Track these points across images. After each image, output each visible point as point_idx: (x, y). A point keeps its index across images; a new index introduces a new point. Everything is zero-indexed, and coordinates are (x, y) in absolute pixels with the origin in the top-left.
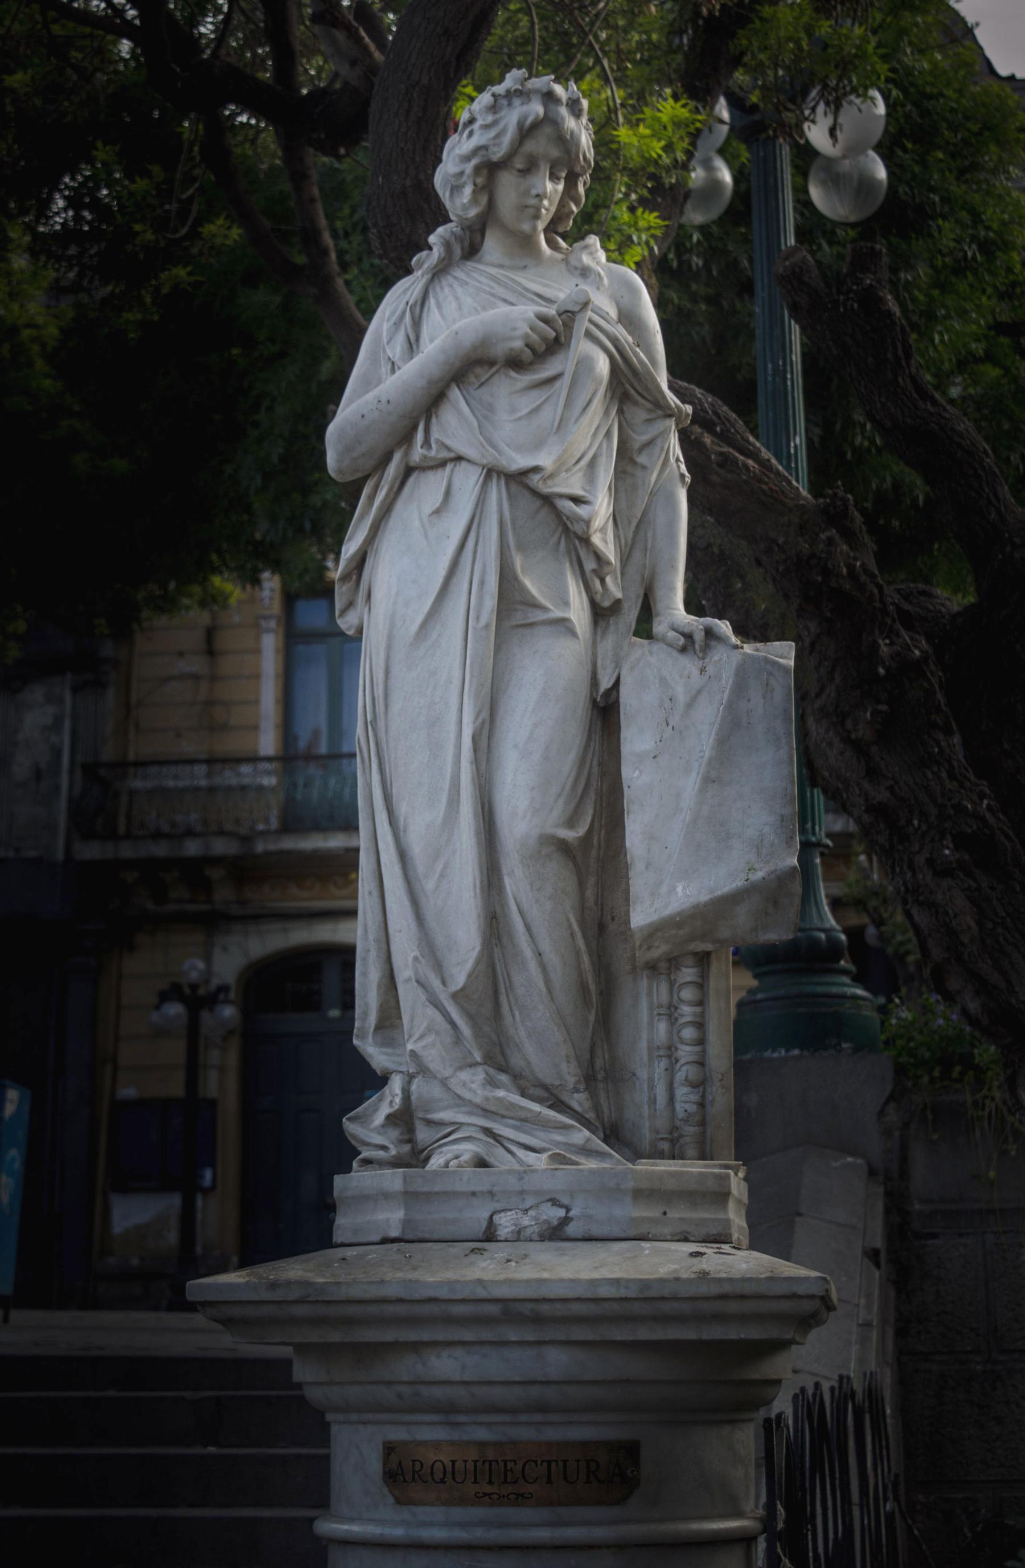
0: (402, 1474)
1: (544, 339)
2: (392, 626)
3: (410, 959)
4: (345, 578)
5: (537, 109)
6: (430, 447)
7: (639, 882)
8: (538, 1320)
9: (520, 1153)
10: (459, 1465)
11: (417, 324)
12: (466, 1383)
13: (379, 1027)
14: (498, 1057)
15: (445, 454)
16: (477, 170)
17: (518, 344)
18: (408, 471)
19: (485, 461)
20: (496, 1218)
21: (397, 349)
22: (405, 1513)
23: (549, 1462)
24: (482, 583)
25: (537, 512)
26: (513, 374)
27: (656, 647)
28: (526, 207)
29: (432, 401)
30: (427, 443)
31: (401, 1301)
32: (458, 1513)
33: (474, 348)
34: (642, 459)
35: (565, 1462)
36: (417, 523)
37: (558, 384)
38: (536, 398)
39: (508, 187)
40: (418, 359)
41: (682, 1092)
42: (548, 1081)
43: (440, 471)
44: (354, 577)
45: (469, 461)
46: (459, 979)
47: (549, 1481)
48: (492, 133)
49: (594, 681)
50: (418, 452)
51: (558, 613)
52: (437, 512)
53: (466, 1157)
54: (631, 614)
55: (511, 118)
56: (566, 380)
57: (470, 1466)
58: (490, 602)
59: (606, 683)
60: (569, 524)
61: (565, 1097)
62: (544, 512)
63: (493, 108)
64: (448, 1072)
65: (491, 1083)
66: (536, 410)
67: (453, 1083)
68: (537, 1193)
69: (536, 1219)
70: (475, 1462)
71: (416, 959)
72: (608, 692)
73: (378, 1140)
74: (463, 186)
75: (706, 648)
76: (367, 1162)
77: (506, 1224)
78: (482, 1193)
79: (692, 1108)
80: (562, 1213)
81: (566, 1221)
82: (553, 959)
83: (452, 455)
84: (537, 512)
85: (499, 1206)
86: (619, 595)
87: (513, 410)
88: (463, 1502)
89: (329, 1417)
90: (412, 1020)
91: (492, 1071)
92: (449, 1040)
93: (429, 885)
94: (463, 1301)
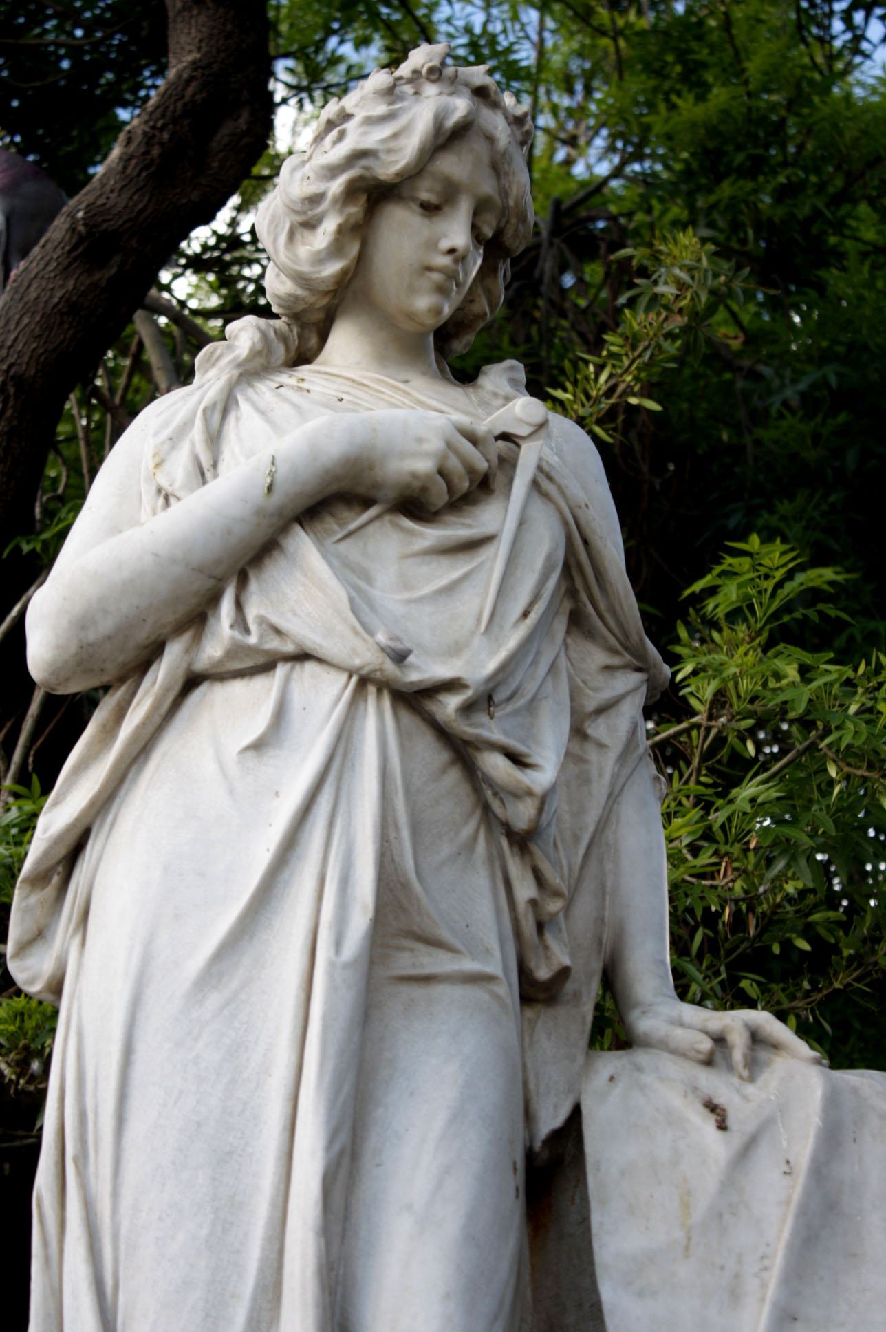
1: (471, 470)
4: (40, 879)
6: (247, 631)
11: (214, 439)
15: (274, 644)
16: (351, 192)
18: (192, 682)
19: (357, 662)
21: (179, 467)
25: (443, 771)
26: (407, 523)
28: (429, 269)
29: (251, 554)
30: (241, 622)
34: (598, 729)
36: (209, 767)
37: (485, 553)
43: (259, 682)
44: (56, 879)
45: (320, 660)
48: (385, 131)
50: (213, 649)
52: (258, 746)
55: (424, 112)
56: (500, 550)
59: (551, 1119)
60: (496, 806)
62: (454, 775)
63: (390, 93)
66: (450, 589)
72: (557, 1136)
74: (311, 225)
75: (753, 1066)
83: (289, 648)
84: (443, 771)
86: (566, 961)
87: (405, 584)
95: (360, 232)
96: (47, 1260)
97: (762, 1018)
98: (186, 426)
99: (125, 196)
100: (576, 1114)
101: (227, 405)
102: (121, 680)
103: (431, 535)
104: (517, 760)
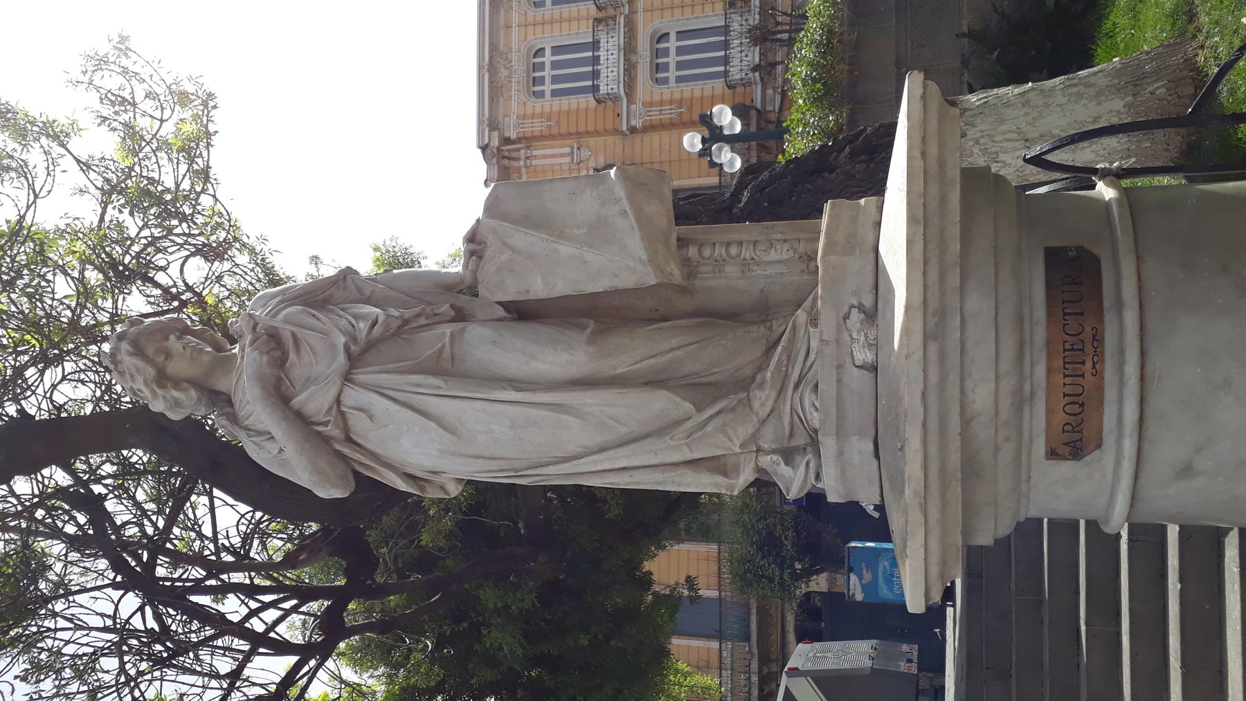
0: (1074, 441)
3: (672, 443)
4: (422, 489)
5: (125, 346)
7: (627, 281)
8: (942, 313)
9: (812, 357)
10: (1068, 390)
11: (260, 433)
12: (997, 378)
13: (725, 475)
14: (744, 384)
16: (162, 386)
17: (265, 358)
18: (349, 440)
20: (858, 363)
22: (1109, 439)
23: (1065, 314)
24: (418, 385)
27: (480, 279)
29: (301, 421)
30: (326, 424)
31: (924, 425)
32: (1110, 393)
33: (264, 388)
34: (367, 293)
35: (1064, 302)
37: (299, 335)
38: (305, 348)
39: (177, 367)
40: (276, 432)
41: (773, 256)
42: (763, 348)
43: (348, 416)
45: (339, 395)
46: (688, 406)
47: (1082, 314)
49: (500, 320)
51: (447, 340)
52: (371, 417)
53: (813, 396)
54: (464, 301)
57: (1068, 380)
58: (431, 380)
59: (501, 312)
61: (775, 336)
64: (755, 419)
65: (761, 386)
67: (763, 413)
68: (838, 330)
69: (859, 332)
70: (1065, 376)
71: (671, 438)
73: (802, 469)
77: (863, 355)
78: (838, 374)
79: (786, 246)
80: (855, 311)
81: (861, 308)
82: (674, 342)
85: (849, 361)
88: (1100, 388)
89: (1022, 519)
90: (718, 447)
91: (754, 385)
92: (730, 416)
93: (623, 430)
94: (925, 371)
95: (177, 383)
98: (254, 443)
100: (498, 303)
101: (246, 429)
102: (348, 464)
103: (292, 356)
104: (375, 323)
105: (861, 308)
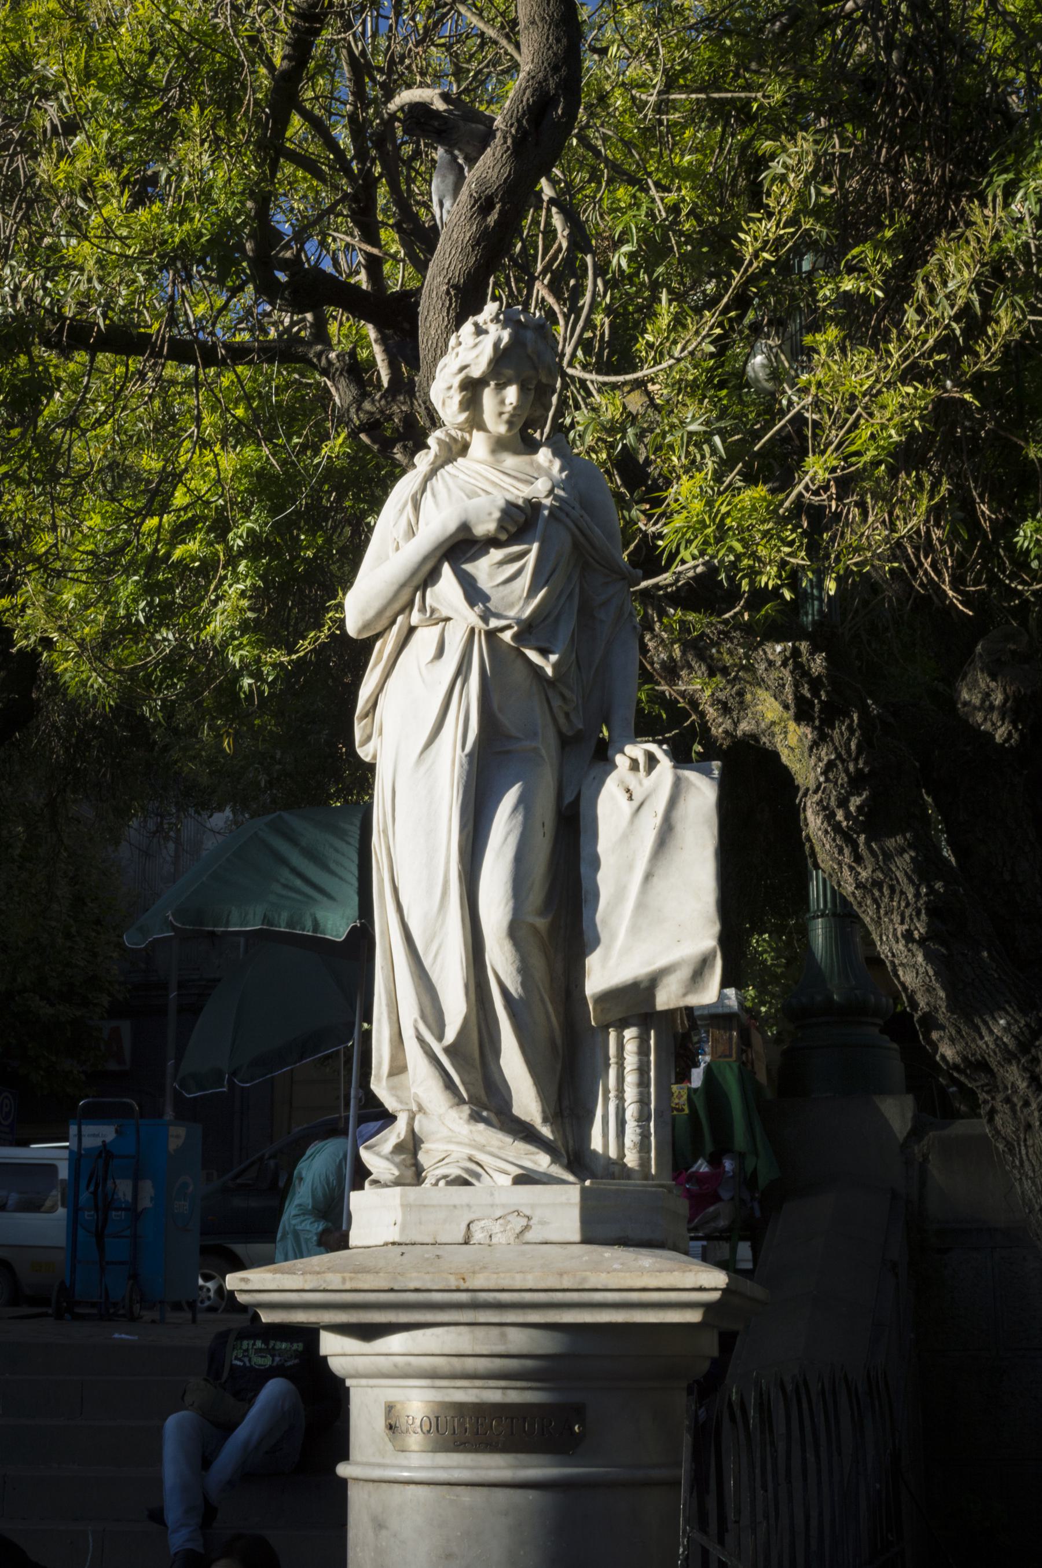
2: (397, 754)
9: (495, 1175)
13: (392, 1074)
38: (512, 569)
46: (451, 1035)
59: (569, 798)
68: (504, 1206)
71: (416, 1021)
76: (376, 1182)
80: (524, 1222)
81: (527, 1228)
85: (472, 1217)
86: (581, 726)
89: (349, 1382)
96: (379, 869)
97: (653, 747)
99: (496, 170)
105: (527, 1228)
